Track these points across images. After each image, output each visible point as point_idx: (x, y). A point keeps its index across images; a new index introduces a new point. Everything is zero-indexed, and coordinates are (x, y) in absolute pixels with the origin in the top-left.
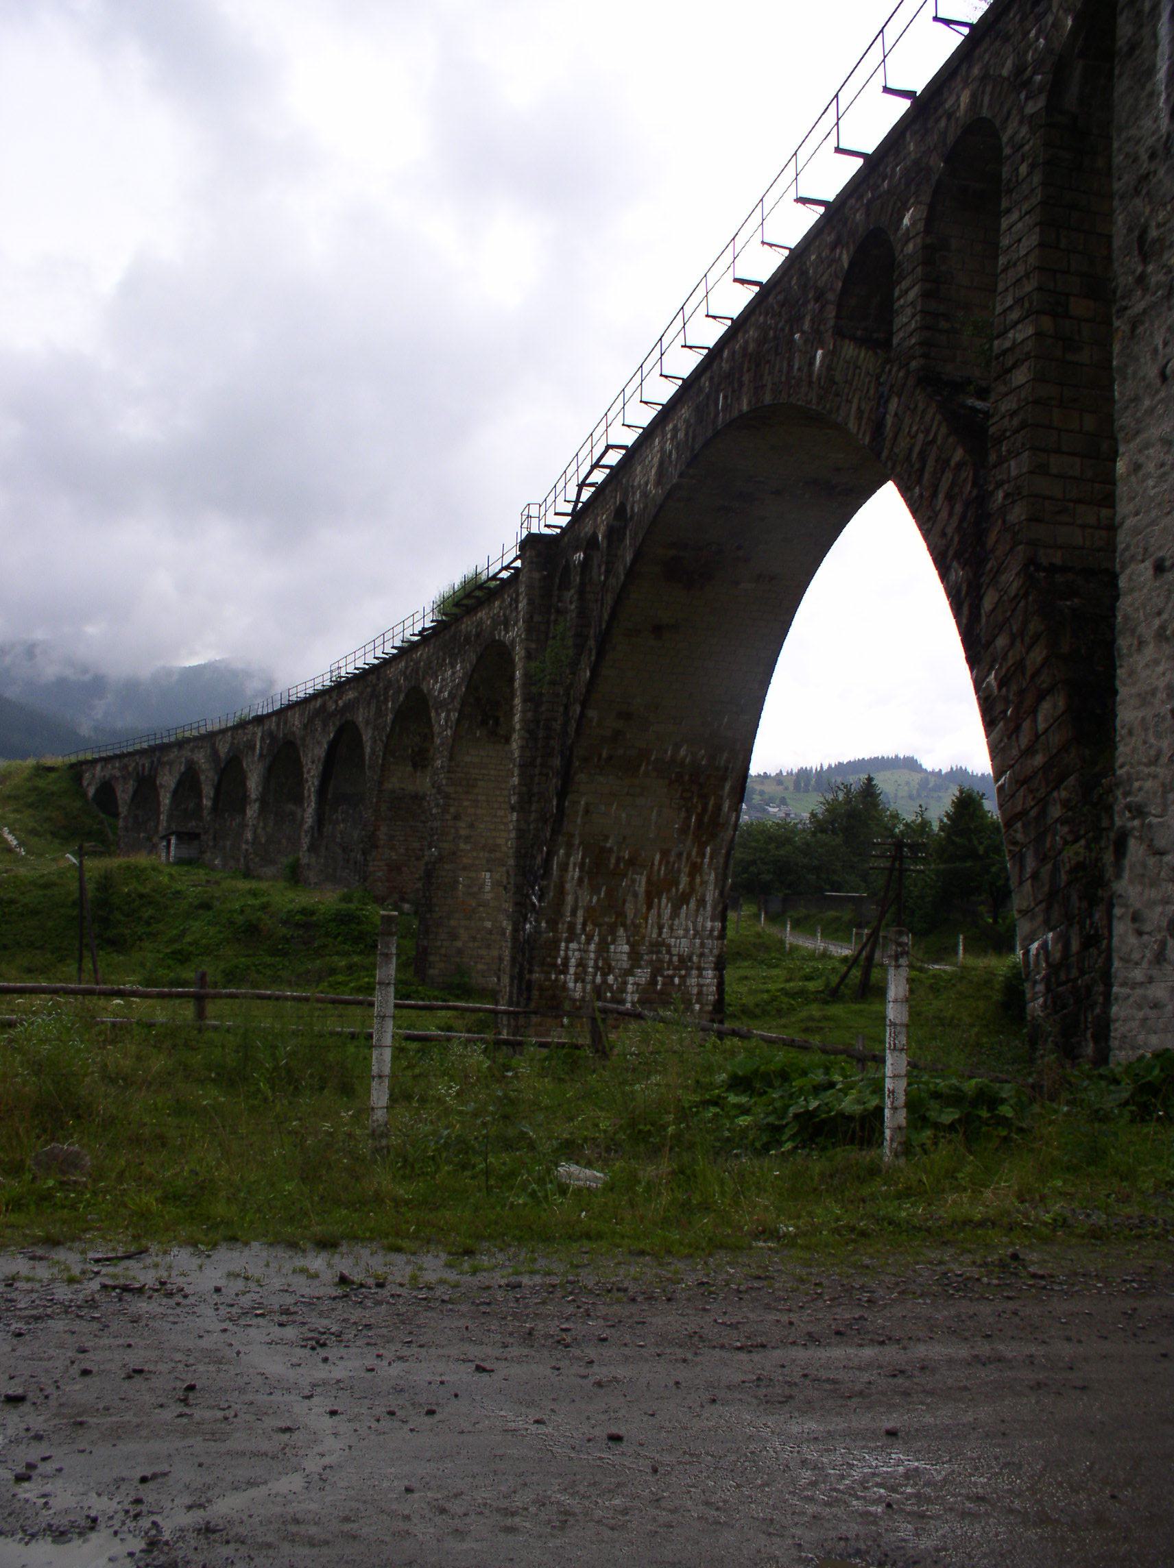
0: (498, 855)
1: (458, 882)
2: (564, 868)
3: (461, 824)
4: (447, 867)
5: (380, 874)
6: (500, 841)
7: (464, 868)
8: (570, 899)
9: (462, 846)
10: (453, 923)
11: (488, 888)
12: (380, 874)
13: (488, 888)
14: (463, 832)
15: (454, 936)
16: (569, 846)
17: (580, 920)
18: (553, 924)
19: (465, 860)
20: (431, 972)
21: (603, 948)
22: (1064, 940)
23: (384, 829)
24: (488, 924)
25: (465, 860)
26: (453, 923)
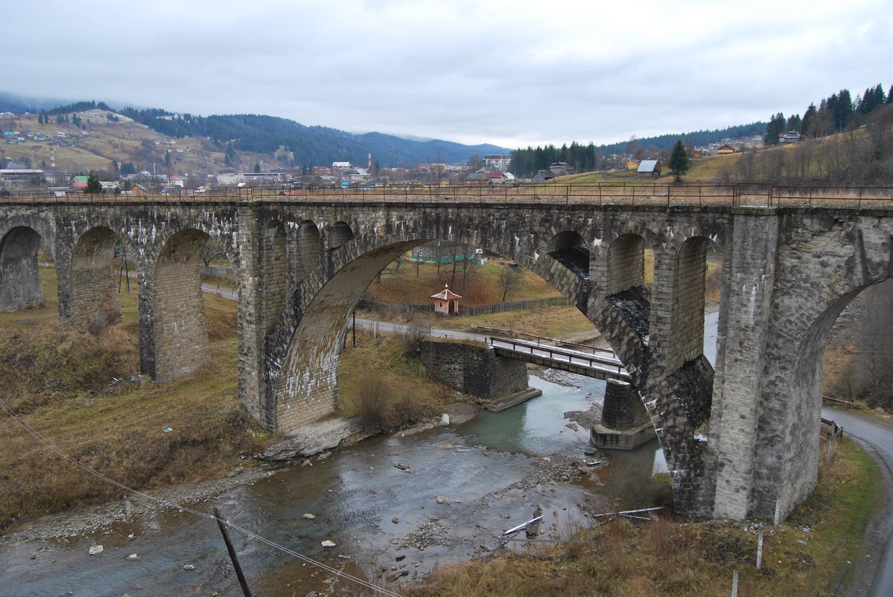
0: (178, 313)
1: (163, 329)
2: (291, 351)
3: (161, 303)
4: (159, 323)
5: (77, 313)
6: (179, 307)
7: (166, 323)
8: (292, 362)
9: (164, 313)
10: (164, 348)
11: (176, 329)
12: (77, 313)
13: (176, 329)
14: (163, 306)
15: (165, 354)
16: (295, 343)
17: (294, 368)
18: (285, 372)
19: (165, 319)
20: (158, 372)
21: (301, 376)
22: (689, 474)
23: (75, 290)
24: (178, 345)
25: (165, 319)
26: (164, 348)
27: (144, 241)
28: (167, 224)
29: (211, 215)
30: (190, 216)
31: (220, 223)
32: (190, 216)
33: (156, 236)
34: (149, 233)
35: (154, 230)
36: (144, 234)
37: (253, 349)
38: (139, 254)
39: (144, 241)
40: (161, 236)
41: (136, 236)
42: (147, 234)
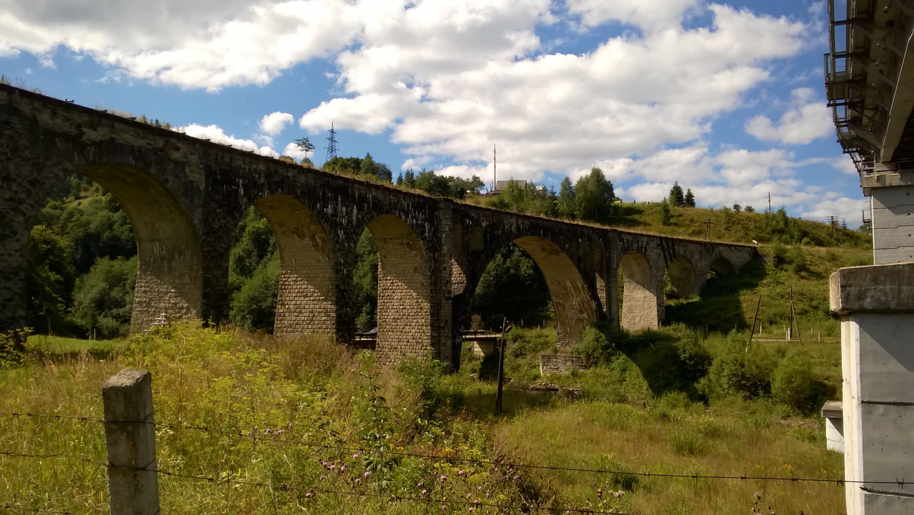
27: (344, 222)
28: (369, 206)
29: (408, 205)
30: (390, 202)
31: (415, 213)
32: (390, 202)
33: (357, 218)
34: (349, 214)
35: (355, 210)
36: (344, 214)
37: (449, 322)
38: (339, 236)
39: (344, 222)
40: (363, 218)
41: (335, 214)
42: (347, 213)
